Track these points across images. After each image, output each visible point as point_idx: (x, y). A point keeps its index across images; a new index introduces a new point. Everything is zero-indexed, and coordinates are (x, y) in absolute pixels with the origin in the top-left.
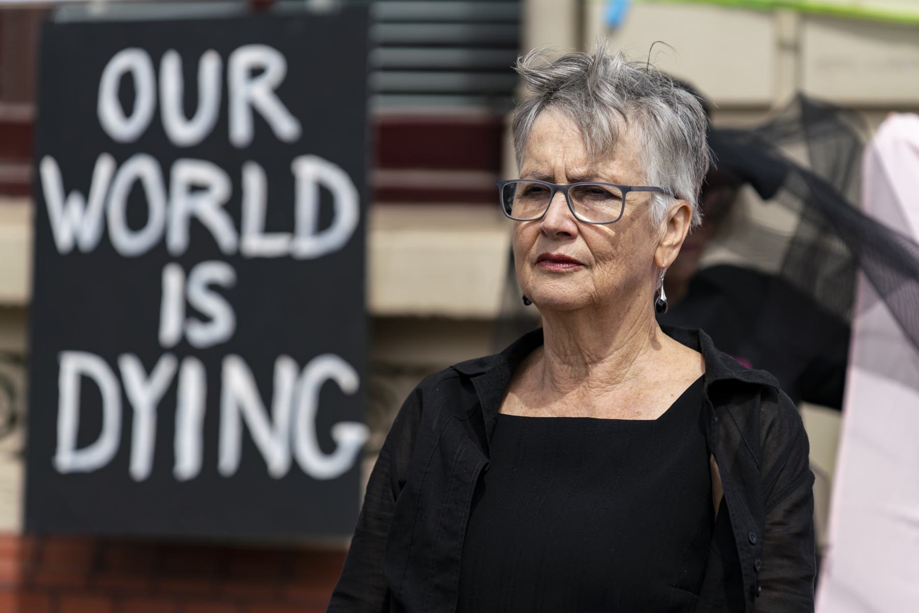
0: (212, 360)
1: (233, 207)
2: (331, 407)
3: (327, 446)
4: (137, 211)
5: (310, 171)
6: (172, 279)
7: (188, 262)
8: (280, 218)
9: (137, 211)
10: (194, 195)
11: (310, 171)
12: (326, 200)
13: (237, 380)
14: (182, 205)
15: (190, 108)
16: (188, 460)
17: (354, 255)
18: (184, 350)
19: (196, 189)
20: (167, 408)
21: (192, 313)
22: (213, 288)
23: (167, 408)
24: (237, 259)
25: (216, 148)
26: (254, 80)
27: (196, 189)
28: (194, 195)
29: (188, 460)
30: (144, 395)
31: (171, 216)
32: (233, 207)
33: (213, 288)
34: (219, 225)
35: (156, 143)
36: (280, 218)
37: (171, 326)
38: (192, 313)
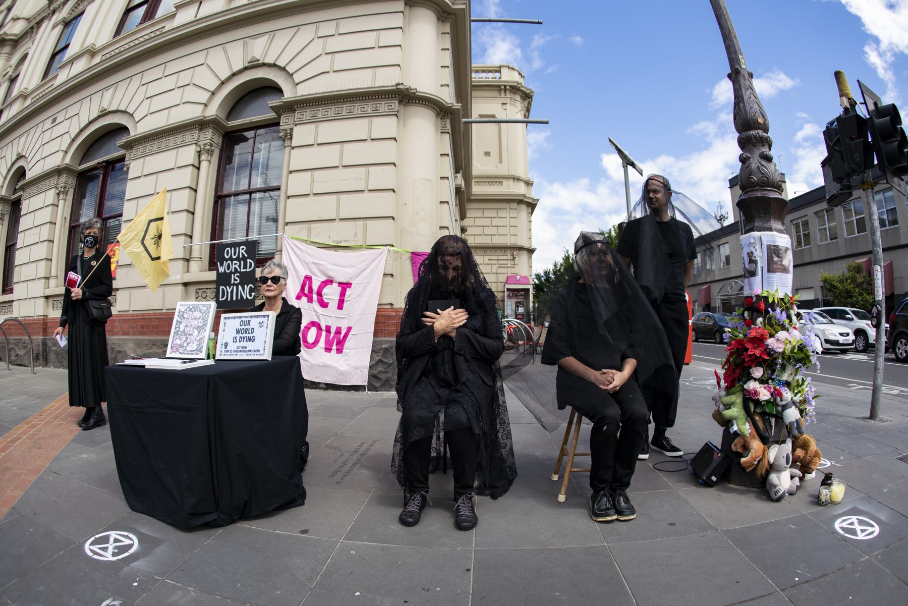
2: (251, 290)
3: (251, 295)
5: (249, 260)
7: (234, 273)
8: (245, 267)
10: (235, 265)
11: (249, 260)
13: (240, 287)
17: (254, 271)
18: (234, 284)
25: (238, 259)
28: (235, 265)
30: (229, 291)
31: (232, 268)
35: (231, 259)
36: (245, 267)
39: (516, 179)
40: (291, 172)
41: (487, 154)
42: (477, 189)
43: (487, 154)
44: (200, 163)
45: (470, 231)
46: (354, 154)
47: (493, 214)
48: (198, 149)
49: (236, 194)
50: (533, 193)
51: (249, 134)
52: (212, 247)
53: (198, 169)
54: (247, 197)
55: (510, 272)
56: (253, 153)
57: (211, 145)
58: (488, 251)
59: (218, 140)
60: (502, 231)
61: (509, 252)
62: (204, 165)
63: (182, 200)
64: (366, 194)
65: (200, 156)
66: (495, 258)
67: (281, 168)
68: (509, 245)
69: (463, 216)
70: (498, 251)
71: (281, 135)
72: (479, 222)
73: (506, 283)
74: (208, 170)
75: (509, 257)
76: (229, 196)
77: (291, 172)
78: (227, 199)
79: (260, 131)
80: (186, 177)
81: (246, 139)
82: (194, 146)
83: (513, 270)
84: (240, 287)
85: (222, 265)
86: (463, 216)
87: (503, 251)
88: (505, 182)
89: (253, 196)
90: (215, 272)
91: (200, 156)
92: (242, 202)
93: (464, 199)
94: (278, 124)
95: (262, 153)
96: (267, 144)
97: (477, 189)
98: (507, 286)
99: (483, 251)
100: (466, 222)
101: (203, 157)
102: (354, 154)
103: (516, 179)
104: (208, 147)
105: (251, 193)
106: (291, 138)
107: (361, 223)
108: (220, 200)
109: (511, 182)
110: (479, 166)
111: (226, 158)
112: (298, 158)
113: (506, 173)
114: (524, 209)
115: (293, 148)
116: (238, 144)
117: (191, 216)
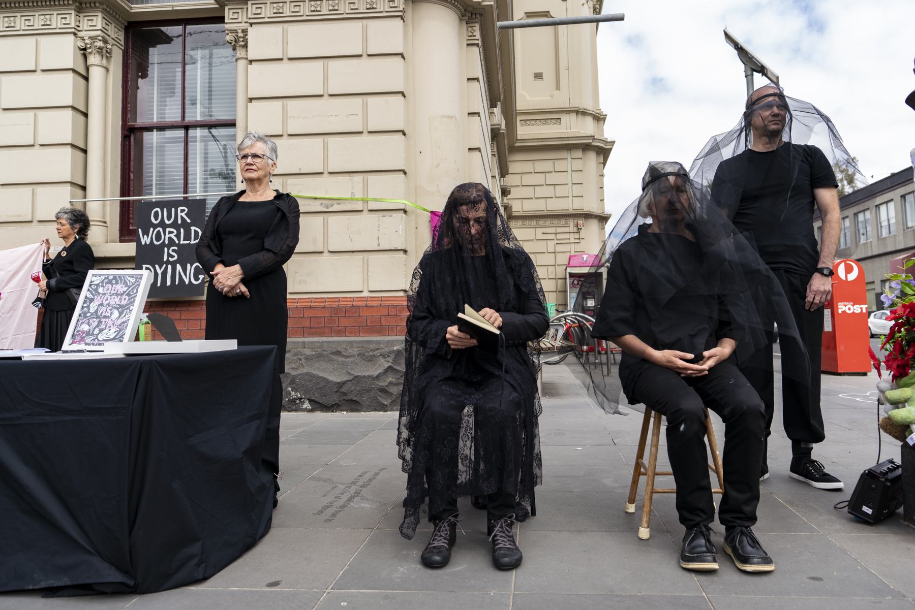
0: (174, 265)
1: (178, 236)
3: (197, 279)
4: (158, 237)
5: (193, 228)
6: (166, 249)
7: (169, 247)
8: (187, 237)
9: (158, 237)
10: (170, 234)
11: (193, 228)
12: (196, 232)
13: (179, 267)
14: (167, 236)
15: (169, 219)
16: (169, 283)
18: (168, 262)
19: (170, 232)
20: (164, 273)
21: (169, 255)
22: (173, 251)
23: (164, 273)
24: (179, 245)
25: (175, 225)
26: (182, 213)
27: (170, 232)
28: (170, 234)
29: (169, 283)
30: (159, 271)
32: (178, 236)
33: (173, 251)
34: (175, 239)
35: (162, 224)
36: (187, 237)
37: (165, 259)
38: (169, 255)
39: (581, 112)
40: (251, 100)
41: (538, 76)
42: (525, 132)
43: (538, 76)
44: (87, 69)
45: (514, 193)
46: (344, 76)
47: (548, 166)
48: (81, 44)
49: (162, 128)
50: (609, 132)
51: (173, 31)
52: (125, 206)
53: (86, 79)
54: (181, 133)
55: (573, 249)
56: (184, 64)
57: (105, 41)
58: (541, 222)
59: (116, 34)
60: (560, 191)
61: (571, 222)
62: (96, 74)
63: (62, 126)
64: (365, 138)
65: (85, 57)
66: (552, 230)
67: (234, 95)
68: (571, 211)
69: (504, 172)
70: (555, 222)
71: (228, 38)
72: (527, 180)
73: (568, 265)
74: (105, 82)
75: (572, 228)
76: (149, 129)
77: (251, 100)
78: (146, 136)
79: (190, 28)
80: (64, 89)
81: (168, 40)
82: (72, 37)
83: (578, 248)
84: (179, 267)
85: (146, 233)
86: (504, 172)
87: (563, 222)
88: (565, 118)
89: (191, 132)
90: (133, 245)
91: (85, 57)
92: (174, 141)
93: (504, 145)
94: (221, 20)
95: (199, 65)
96: (207, 52)
97: (525, 132)
98: (569, 270)
99: (534, 222)
100: (509, 180)
101: (94, 59)
102: (344, 76)
103: (581, 112)
104: (101, 44)
105: (187, 128)
106: (246, 46)
107: (358, 178)
108: (132, 134)
109: (573, 116)
110: (528, 95)
111: (135, 68)
112: (260, 79)
113: (566, 105)
114: (592, 159)
115: (251, 62)
116: (154, 46)
117: (81, 155)
